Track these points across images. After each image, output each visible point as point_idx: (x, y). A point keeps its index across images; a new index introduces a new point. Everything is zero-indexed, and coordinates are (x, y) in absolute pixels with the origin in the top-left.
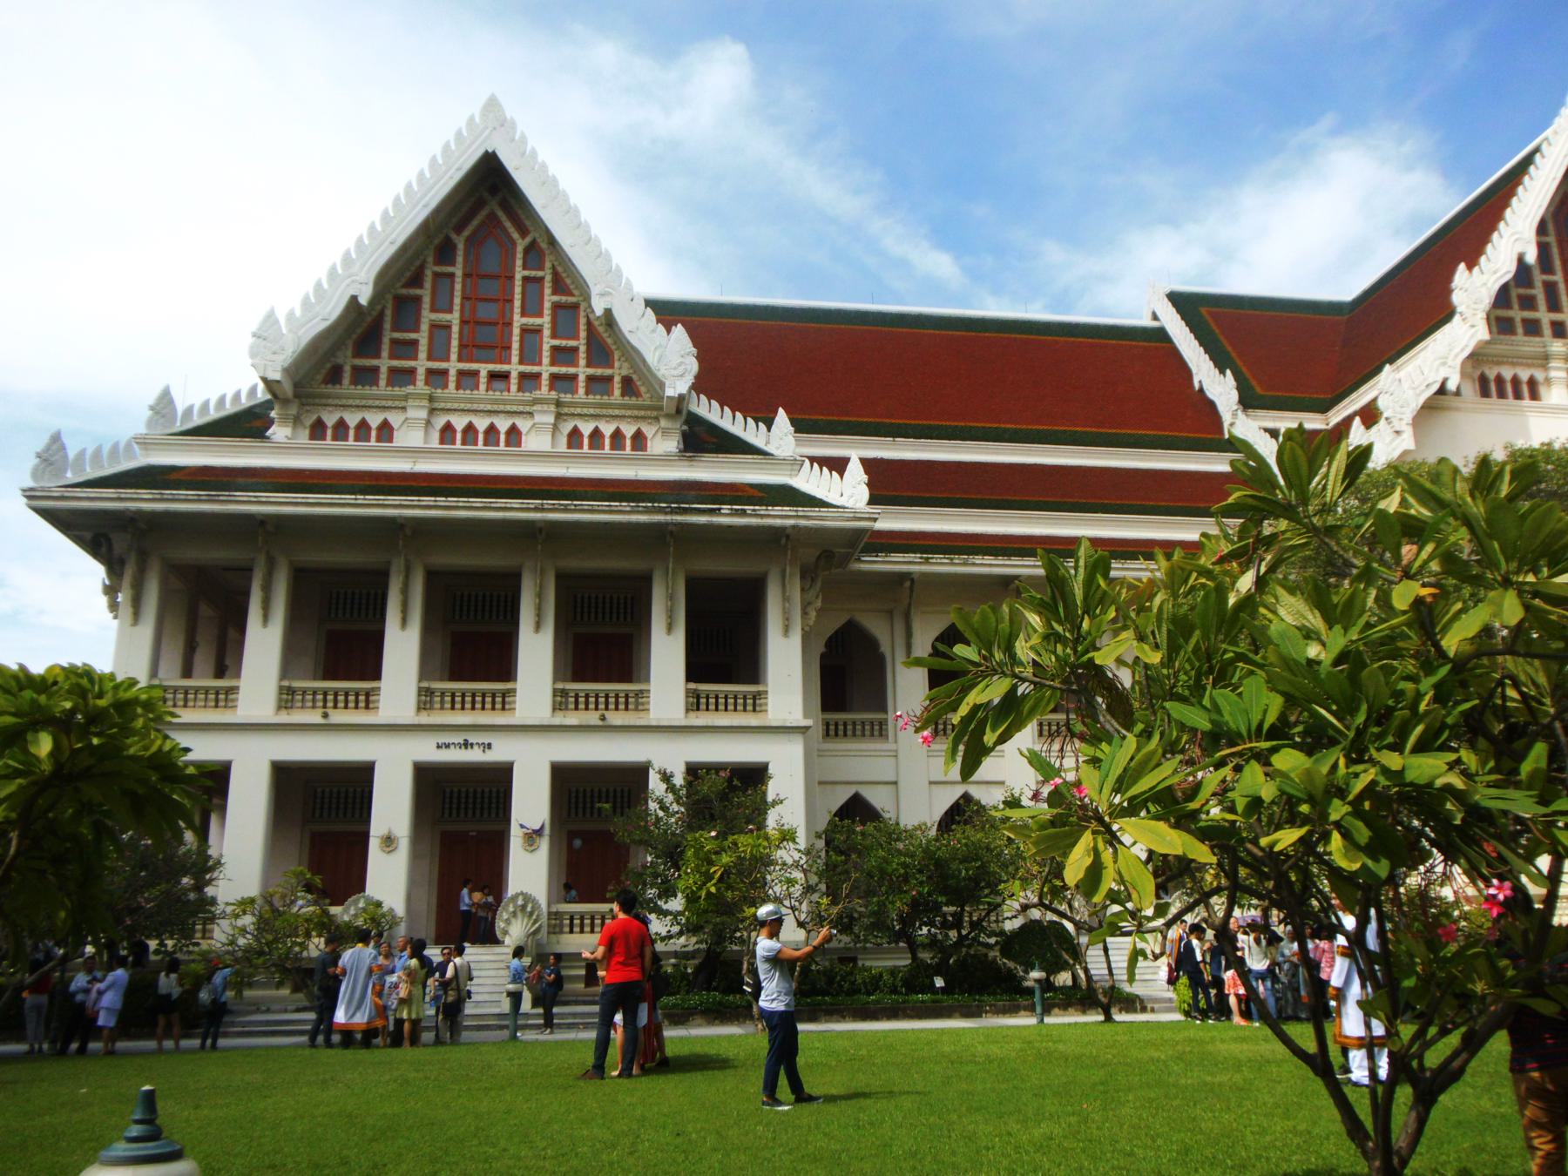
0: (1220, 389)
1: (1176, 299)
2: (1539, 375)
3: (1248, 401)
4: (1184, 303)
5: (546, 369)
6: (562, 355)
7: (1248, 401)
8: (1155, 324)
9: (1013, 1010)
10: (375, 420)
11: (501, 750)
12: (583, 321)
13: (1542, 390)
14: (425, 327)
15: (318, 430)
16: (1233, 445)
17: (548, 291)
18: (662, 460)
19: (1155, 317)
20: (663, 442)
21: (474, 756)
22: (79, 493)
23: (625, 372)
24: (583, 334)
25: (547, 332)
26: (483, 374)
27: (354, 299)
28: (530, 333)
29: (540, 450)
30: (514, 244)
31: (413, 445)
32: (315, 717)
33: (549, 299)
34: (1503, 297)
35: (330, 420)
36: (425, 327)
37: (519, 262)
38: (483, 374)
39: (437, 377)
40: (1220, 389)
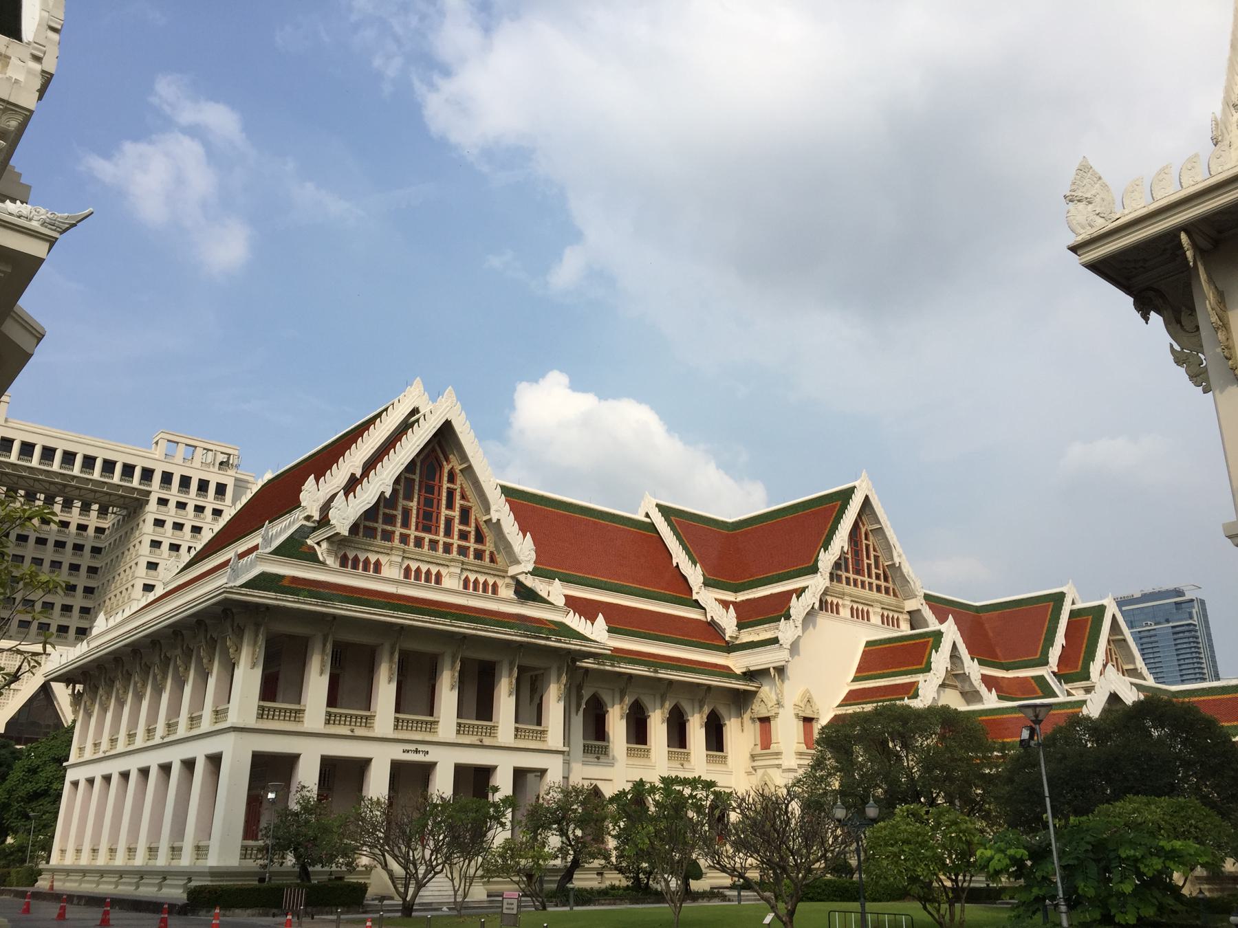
0: (694, 575)
1: (665, 511)
2: (840, 602)
3: (707, 584)
4: (665, 511)
5: (456, 541)
6: (464, 536)
7: (707, 584)
8: (647, 520)
9: (659, 902)
10: (373, 558)
11: (434, 755)
12: (473, 518)
13: (841, 609)
14: (400, 508)
15: (344, 562)
16: (696, 605)
17: (458, 497)
18: (506, 603)
19: (647, 515)
20: (507, 592)
21: (419, 758)
22: (244, 591)
23: (493, 549)
24: (473, 525)
25: (457, 521)
26: (427, 540)
27: (383, 493)
28: (449, 521)
29: (451, 587)
30: (441, 467)
31: (390, 574)
32: (345, 730)
33: (458, 502)
34: (837, 565)
35: (351, 555)
36: (400, 508)
37: (445, 479)
38: (427, 540)
39: (404, 539)
40: (694, 575)
